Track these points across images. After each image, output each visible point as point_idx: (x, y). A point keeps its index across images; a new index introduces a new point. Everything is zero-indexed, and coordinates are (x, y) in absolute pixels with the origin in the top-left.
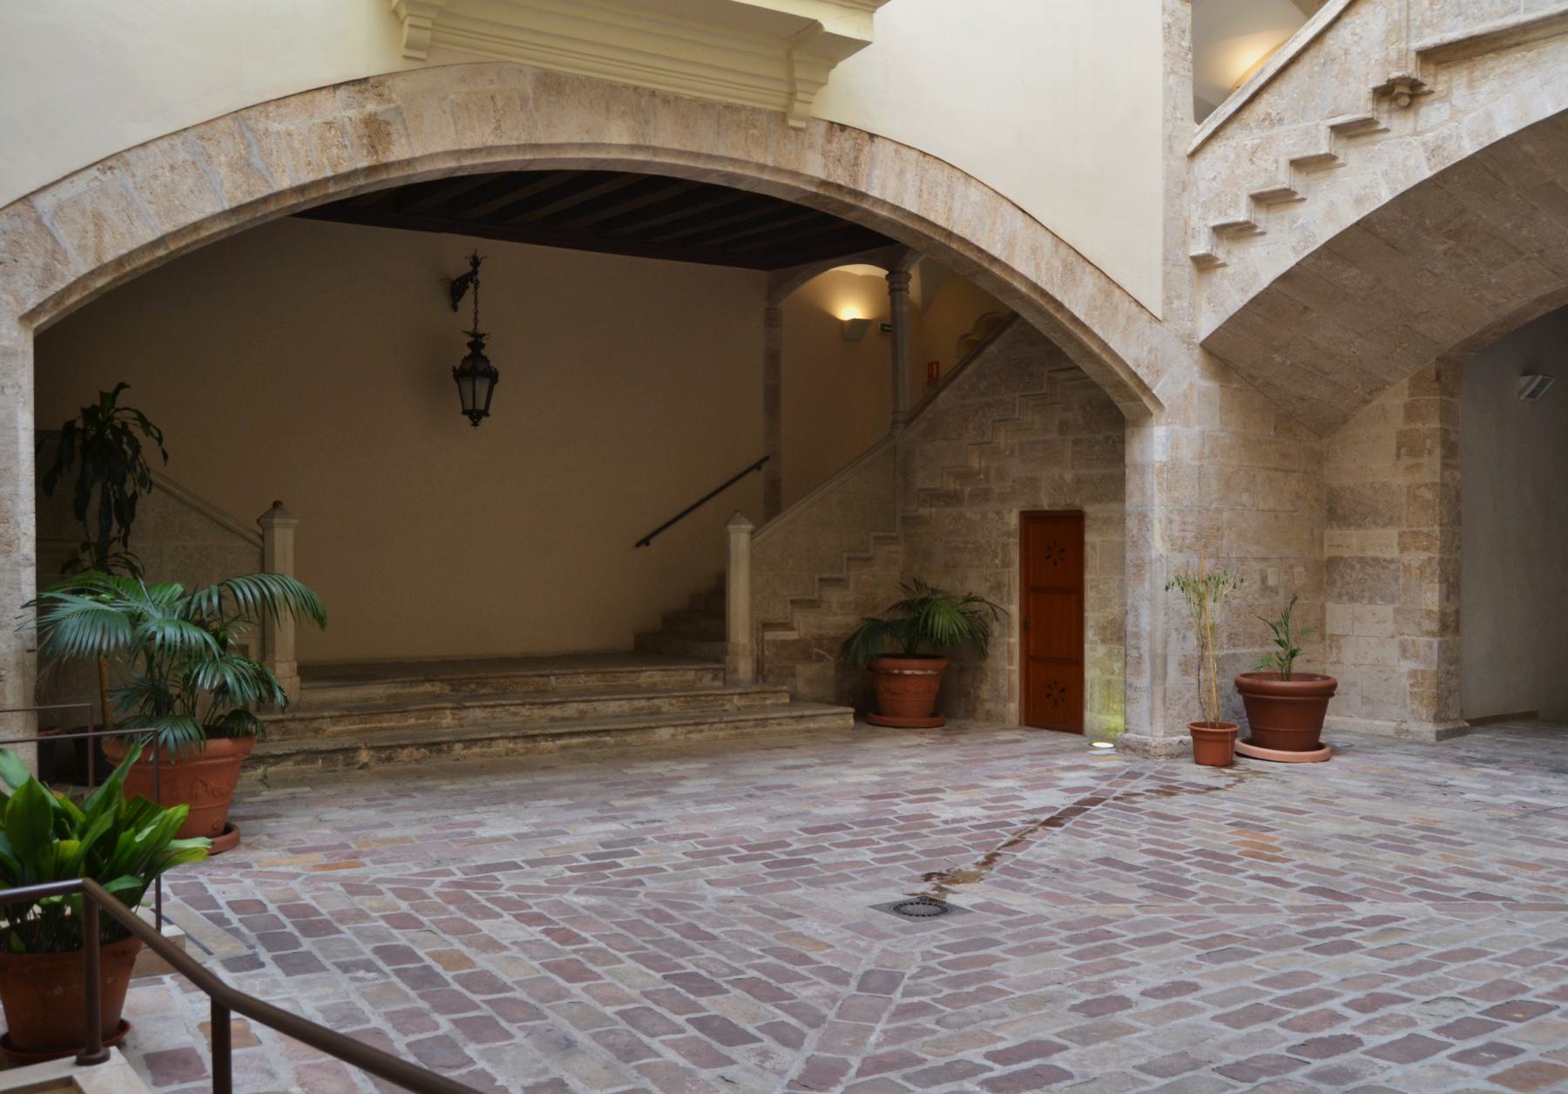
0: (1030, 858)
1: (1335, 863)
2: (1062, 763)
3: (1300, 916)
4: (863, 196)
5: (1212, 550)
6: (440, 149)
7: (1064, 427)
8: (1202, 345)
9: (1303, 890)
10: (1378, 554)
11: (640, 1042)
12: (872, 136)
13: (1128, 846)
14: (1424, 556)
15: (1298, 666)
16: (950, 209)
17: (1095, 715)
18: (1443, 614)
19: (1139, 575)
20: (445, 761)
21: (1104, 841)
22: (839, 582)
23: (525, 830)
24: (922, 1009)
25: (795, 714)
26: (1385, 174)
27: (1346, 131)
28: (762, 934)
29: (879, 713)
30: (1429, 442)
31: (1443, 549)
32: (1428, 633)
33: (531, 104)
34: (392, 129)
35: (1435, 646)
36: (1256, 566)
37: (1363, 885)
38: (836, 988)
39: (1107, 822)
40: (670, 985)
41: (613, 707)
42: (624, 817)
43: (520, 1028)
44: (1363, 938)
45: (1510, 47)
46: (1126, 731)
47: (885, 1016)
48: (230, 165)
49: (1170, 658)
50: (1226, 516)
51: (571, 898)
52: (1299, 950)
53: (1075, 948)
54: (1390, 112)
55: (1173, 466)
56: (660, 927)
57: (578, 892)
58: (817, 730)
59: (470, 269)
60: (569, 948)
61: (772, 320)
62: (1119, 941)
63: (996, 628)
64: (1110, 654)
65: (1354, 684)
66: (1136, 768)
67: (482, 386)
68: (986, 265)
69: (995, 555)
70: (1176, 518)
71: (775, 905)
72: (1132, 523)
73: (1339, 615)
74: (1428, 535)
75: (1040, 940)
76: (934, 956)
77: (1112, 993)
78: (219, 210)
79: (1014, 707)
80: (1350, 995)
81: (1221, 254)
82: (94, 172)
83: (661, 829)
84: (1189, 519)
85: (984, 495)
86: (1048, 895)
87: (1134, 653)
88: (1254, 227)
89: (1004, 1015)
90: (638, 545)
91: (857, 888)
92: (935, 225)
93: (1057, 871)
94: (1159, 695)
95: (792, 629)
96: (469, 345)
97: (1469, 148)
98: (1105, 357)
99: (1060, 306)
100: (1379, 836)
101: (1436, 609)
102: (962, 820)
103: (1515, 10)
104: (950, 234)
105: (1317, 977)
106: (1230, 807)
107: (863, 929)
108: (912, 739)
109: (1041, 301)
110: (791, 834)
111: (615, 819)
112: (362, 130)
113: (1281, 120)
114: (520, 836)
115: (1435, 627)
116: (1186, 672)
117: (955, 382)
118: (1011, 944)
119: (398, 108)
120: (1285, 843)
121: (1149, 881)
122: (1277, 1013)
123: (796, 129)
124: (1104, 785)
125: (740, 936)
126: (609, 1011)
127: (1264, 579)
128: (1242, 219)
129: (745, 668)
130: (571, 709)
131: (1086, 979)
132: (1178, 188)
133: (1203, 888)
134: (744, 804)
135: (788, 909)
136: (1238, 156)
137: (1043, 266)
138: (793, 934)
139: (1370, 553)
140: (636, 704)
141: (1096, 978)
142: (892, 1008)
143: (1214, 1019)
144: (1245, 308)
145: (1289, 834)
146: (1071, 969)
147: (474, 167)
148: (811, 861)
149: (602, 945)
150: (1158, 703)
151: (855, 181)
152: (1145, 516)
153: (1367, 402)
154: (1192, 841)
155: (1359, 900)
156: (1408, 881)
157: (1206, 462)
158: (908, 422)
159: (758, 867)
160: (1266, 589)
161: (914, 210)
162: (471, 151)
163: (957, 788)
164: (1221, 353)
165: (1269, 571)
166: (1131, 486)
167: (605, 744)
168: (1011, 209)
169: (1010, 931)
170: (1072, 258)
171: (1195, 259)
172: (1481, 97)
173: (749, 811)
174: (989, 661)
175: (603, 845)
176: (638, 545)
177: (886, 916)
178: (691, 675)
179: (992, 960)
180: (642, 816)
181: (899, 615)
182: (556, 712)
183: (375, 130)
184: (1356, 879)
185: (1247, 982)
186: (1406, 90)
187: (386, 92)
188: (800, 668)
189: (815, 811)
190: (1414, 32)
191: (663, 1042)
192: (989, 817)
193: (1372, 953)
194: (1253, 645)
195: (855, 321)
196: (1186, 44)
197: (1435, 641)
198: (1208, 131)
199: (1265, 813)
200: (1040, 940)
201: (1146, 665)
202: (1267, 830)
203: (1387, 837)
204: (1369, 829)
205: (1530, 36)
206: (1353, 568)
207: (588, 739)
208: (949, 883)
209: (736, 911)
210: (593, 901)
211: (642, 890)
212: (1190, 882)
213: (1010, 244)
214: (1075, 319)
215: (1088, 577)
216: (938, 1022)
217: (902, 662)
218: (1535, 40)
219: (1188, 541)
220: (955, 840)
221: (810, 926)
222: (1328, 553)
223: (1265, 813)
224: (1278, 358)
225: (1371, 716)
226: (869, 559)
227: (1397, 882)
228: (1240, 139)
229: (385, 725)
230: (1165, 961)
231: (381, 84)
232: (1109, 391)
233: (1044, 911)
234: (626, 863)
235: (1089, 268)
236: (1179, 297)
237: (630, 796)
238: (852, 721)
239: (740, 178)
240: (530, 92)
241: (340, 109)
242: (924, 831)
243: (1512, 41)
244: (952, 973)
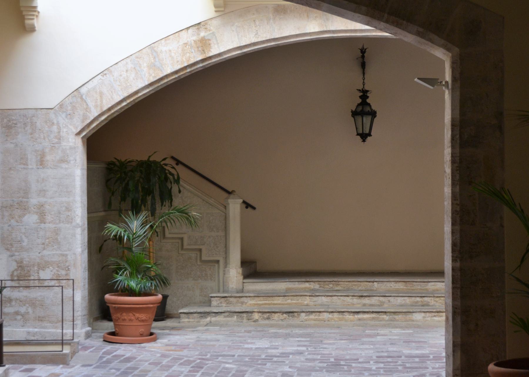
6: (231, 47)
20: (295, 321)
48: (148, 66)
67: (367, 120)
78: (143, 85)
82: (100, 76)
96: (361, 97)
130: (374, 300)
167: (383, 320)
182: (366, 301)
187: (208, 27)
229: (275, 302)
231: (206, 24)
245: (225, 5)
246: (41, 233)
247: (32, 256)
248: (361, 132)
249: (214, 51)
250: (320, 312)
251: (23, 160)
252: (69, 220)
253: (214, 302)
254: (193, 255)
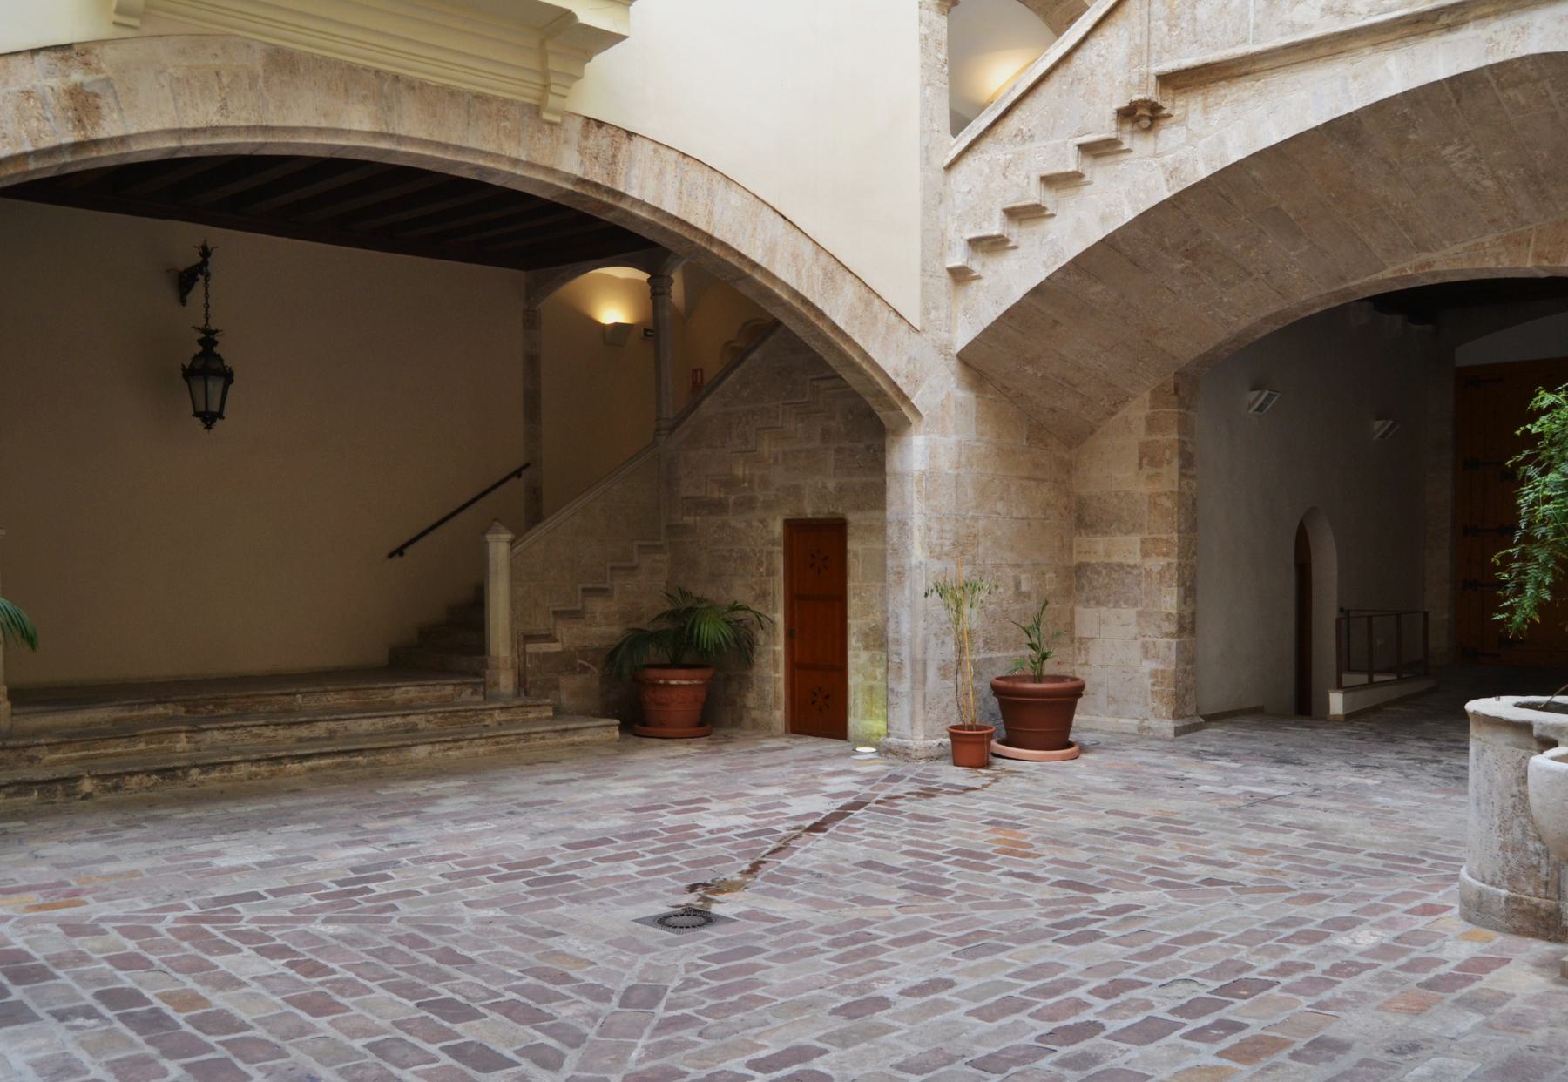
0: (794, 864)
1: (1081, 856)
2: (827, 768)
3: (1050, 909)
4: (622, 196)
5: (968, 557)
6: (157, 127)
7: (826, 435)
8: (960, 356)
9: (1053, 884)
10: (1123, 561)
11: (390, 1074)
12: (630, 134)
13: (888, 848)
14: (1164, 561)
15: (1049, 668)
16: (711, 213)
17: (858, 721)
18: (1181, 616)
19: (900, 582)
21: (866, 844)
22: (603, 592)
23: (269, 857)
24: (685, 1021)
25: (558, 727)
26: (1128, 193)
27: (1092, 150)
28: (523, 954)
29: (645, 724)
30: (1168, 453)
31: (1180, 556)
32: (1167, 635)
33: (261, 83)
34: (101, 103)
35: (1174, 647)
36: (1010, 572)
37: (1106, 877)
38: (597, 1005)
39: (870, 825)
40: (424, 1013)
41: (365, 725)
42: (377, 840)
43: (259, 1069)
44: (1106, 927)
45: (1240, 76)
46: (888, 735)
47: (647, 1031)
49: (929, 663)
50: (982, 524)
51: (317, 928)
52: (1048, 942)
53: (837, 952)
54: (1132, 133)
55: (931, 475)
56: (414, 953)
57: (326, 921)
58: (582, 743)
59: (199, 259)
60: (314, 980)
61: (531, 321)
62: (879, 943)
63: (761, 637)
64: (872, 660)
65: (1100, 685)
66: (898, 771)
67: (215, 387)
68: (747, 270)
69: (760, 564)
70: (935, 526)
71: (536, 924)
72: (892, 531)
73: (1087, 619)
74: (1167, 541)
75: (802, 945)
76: (698, 967)
77: (872, 994)
79: (779, 715)
80: (1094, 983)
81: (976, 267)
83: (417, 850)
84: (947, 527)
85: (747, 504)
86: (811, 901)
87: (895, 659)
88: (1007, 241)
89: (766, 1023)
90: (391, 555)
91: (622, 903)
92: (695, 229)
93: (820, 876)
94: (920, 700)
95: (555, 641)
96: (201, 342)
97: (1203, 172)
98: (865, 366)
99: (821, 314)
100: (1122, 829)
101: (1174, 611)
102: (727, 829)
103: (1245, 41)
104: (711, 239)
105: (1064, 967)
106: (986, 806)
107: (628, 944)
108: (680, 749)
109: (803, 309)
110: (554, 850)
111: (367, 842)
112: (66, 102)
113: (1032, 136)
114: (262, 864)
115: (1173, 628)
116: (944, 677)
117: (719, 389)
118: (774, 951)
119: (107, 80)
120: (1036, 840)
121: (909, 881)
122: (1027, 1004)
123: (552, 124)
124: (867, 789)
125: (500, 957)
126: (358, 1044)
127: (1017, 585)
128: (995, 233)
129: (506, 681)
131: (847, 982)
132: (935, 200)
133: (959, 886)
134: (506, 822)
135: (549, 928)
136: (991, 170)
137: (804, 272)
138: (555, 953)
139: (1115, 559)
140: (389, 721)
141: (857, 980)
142: (655, 1022)
143: (969, 1013)
144: (998, 320)
145: (1040, 831)
146: (833, 973)
147: (198, 148)
148: (574, 877)
149: (351, 975)
150: (919, 706)
151: (613, 180)
152: (905, 524)
153: (1113, 414)
154: (949, 841)
155: (1103, 891)
156: (1147, 871)
157: (962, 471)
158: (672, 430)
159: (519, 885)
160: (1020, 595)
161: (674, 213)
162: (194, 131)
163: (722, 798)
164: (977, 364)
165: (1023, 577)
166: (891, 496)
167: (357, 765)
168: (772, 215)
169: (774, 938)
170: (833, 266)
171: (951, 271)
172: (1214, 123)
173: (510, 828)
174: (755, 670)
175: (354, 870)
176: (391, 555)
177: (650, 929)
178: (449, 690)
179: (756, 968)
180: (396, 837)
181: (665, 625)
183: (82, 103)
184: (1101, 871)
185: (1000, 976)
186: (1147, 113)
187: (94, 61)
188: (563, 681)
189: (579, 826)
190: (1154, 57)
191: (414, 1073)
192: (754, 825)
193: (1115, 942)
194: (1007, 649)
195: (617, 326)
196: (942, 56)
197: (1174, 642)
198: (963, 145)
199: (1019, 811)
200: (802, 945)
201: (907, 671)
202: (1021, 827)
203: (1135, 831)
204: (1114, 822)
205: (1257, 67)
206: (1099, 573)
207: (339, 760)
208: (714, 893)
209: (496, 932)
210: (342, 929)
211: (395, 916)
212: (949, 881)
213: (771, 250)
214: (836, 328)
215: (851, 584)
216: (700, 1034)
217: (669, 673)
218: (1262, 70)
219: (946, 549)
220: (721, 849)
221: (572, 944)
222: (1077, 559)
223: (1019, 811)
224: (1030, 370)
225: (1116, 714)
226: (633, 568)
227: (1138, 872)
228: (994, 153)
230: (923, 960)
231: (87, 52)
232: (869, 400)
233: (808, 916)
234: (378, 888)
235: (849, 277)
236: (936, 308)
237: (384, 818)
238: (617, 733)
239: (493, 172)
240: (259, 69)
241: (40, 77)
242: (690, 842)
243: (1243, 70)
244: (715, 983)
248: (202, 408)
249: (110, 126)
250: (232, 763)
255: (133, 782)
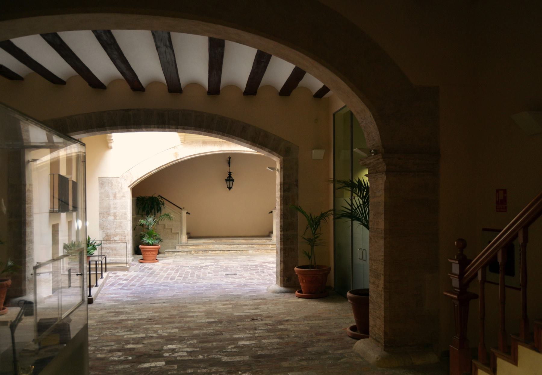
20: (207, 254)
67: (231, 182)
130: (235, 246)
182: (232, 246)
183: (176, 154)
245: (184, 141)
246: (115, 223)
247: (112, 231)
251: (108, 196)
252: (126, 218)
253: (177, 248)
254: (169, 231)
255: (200, 252)
